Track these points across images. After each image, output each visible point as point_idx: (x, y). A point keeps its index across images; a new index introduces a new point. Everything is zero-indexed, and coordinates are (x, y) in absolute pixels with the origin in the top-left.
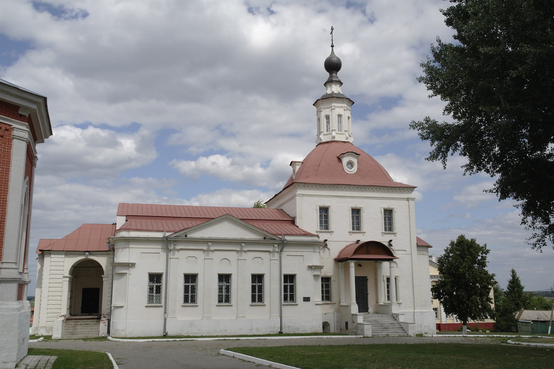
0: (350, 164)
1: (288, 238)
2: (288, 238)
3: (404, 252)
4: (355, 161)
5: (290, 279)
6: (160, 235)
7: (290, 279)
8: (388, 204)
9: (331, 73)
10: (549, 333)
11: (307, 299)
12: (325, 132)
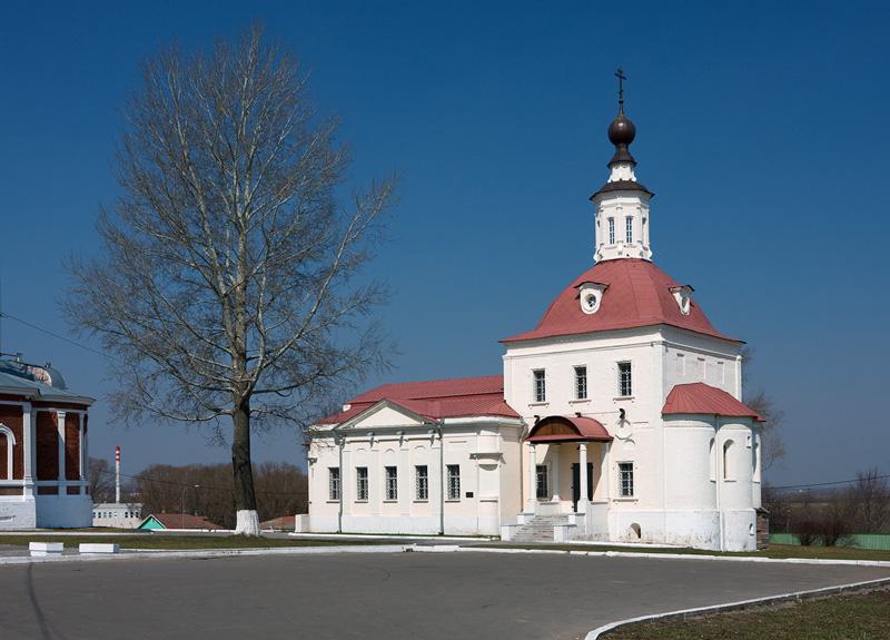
0: (591, 299)
1: (447, 421)
2: (447, 421)
3: (647, 425)
4: (598, 294)
5: (454, 469)
6: (330, 427)
7: (454, 469)
8: (624, 356)
9: (618, 147)
10: (118, 499)
11: (470, 495)
12: (608, 244)
